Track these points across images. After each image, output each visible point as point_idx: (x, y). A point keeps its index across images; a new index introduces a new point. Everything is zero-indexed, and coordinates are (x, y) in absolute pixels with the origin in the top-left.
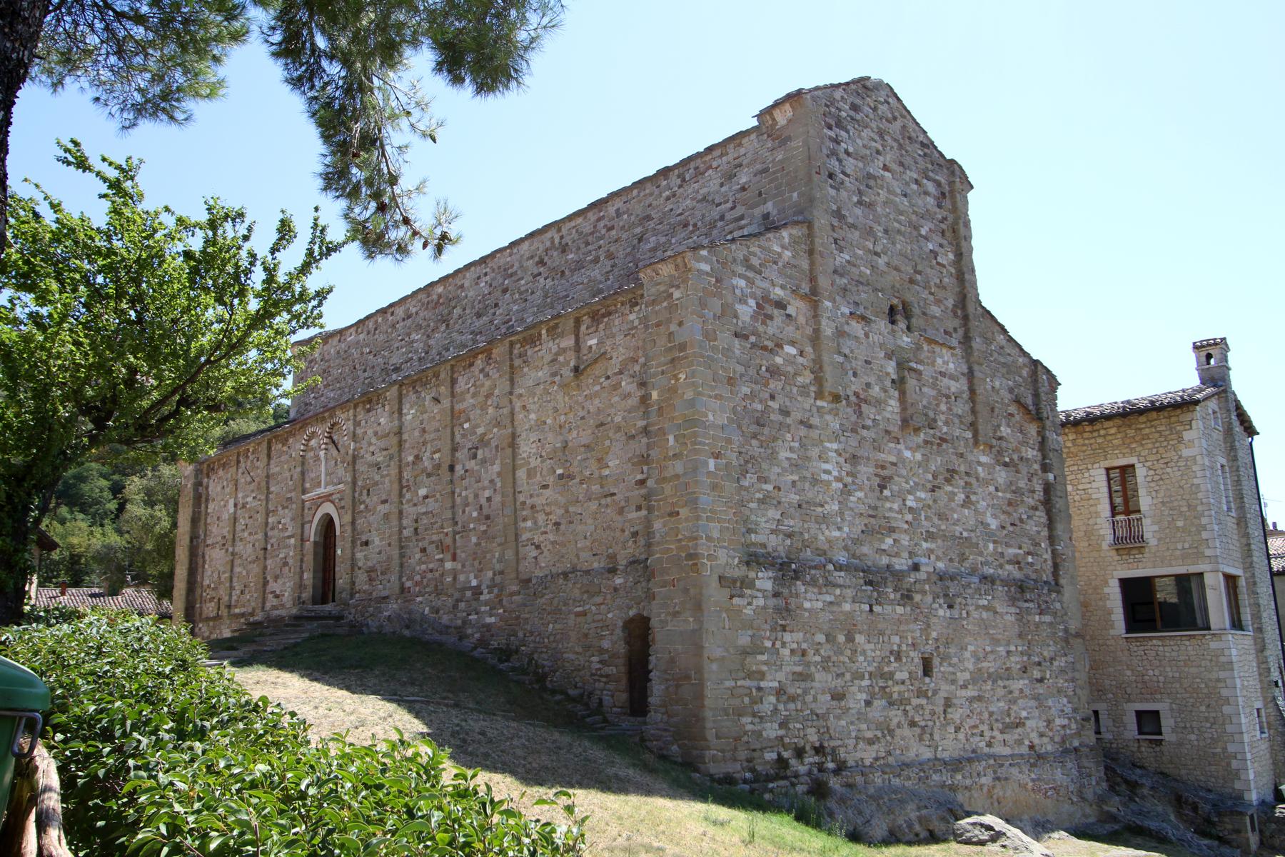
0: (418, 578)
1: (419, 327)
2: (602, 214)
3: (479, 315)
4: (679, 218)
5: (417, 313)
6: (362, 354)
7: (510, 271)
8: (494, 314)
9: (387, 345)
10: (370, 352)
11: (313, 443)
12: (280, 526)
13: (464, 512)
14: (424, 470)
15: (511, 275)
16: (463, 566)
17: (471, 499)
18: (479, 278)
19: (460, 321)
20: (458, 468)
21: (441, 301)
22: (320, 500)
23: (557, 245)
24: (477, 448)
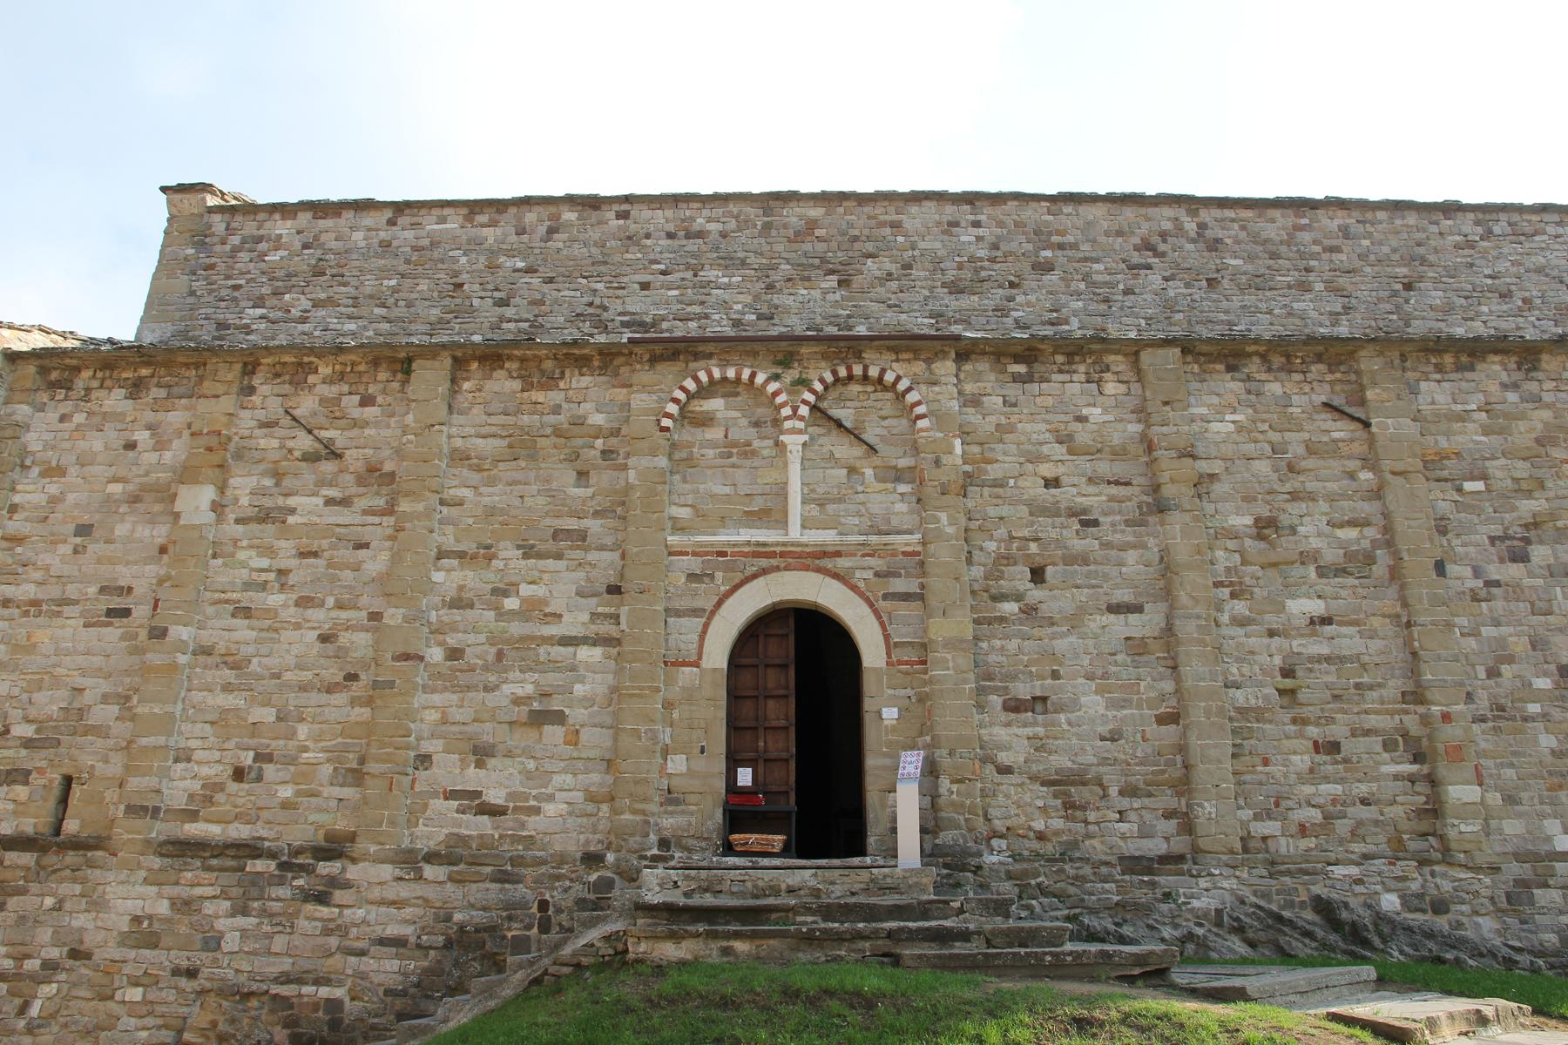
0: (1315, 815)
1: (730, 263)
2: (1304, 221)
3: (955, 289)
4: (1489, 281)
5: (724, 235)
6: (492, 267)
7: (1055, 239)
8: (1011, 299)
9: (603, 269)
10: (530, 270)
11: (715, 404)
12: (511, 603)
13: (1493, 673)
14: (1305, 558)
15: (1061, 247)
16: (1510, 800)
17: (1520, 645)
18: (954, 224)
19: (894, 285)
20: (1459, 572)
21: (818, 232)
22: (764, 563)
23: (1193, 234)
24: (1527, 541)
